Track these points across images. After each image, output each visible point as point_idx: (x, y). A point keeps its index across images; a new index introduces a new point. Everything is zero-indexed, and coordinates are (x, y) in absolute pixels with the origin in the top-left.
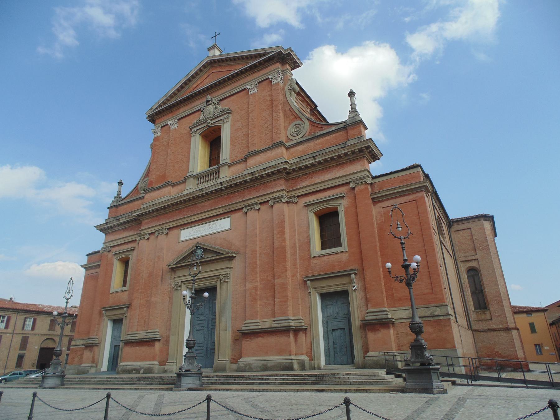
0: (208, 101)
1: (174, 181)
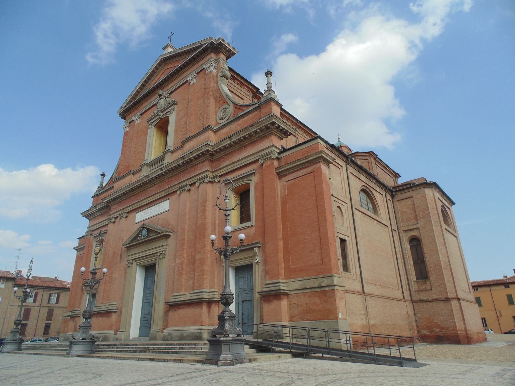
0: (160, 96)
1: (135, 169)
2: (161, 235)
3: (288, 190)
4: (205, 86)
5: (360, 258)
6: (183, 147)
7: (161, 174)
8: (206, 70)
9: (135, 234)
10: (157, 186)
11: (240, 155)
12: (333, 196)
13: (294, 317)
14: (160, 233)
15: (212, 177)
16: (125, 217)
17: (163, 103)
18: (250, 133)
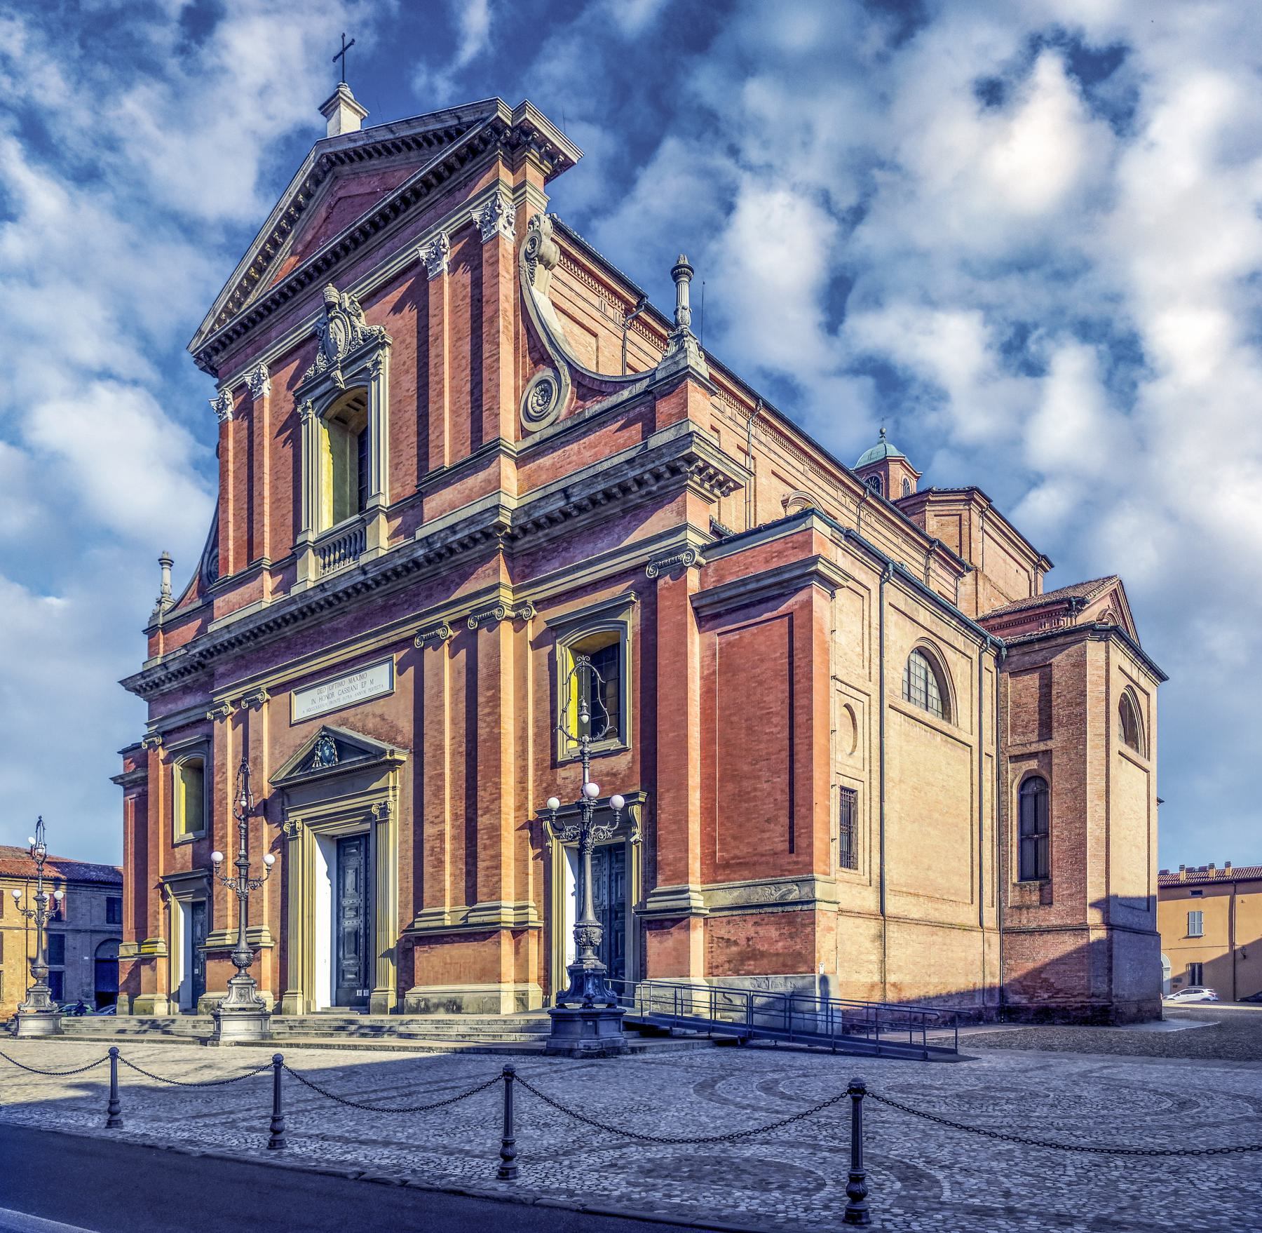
3: (720, 658)
5: (886, 834)
13: (717, 967)
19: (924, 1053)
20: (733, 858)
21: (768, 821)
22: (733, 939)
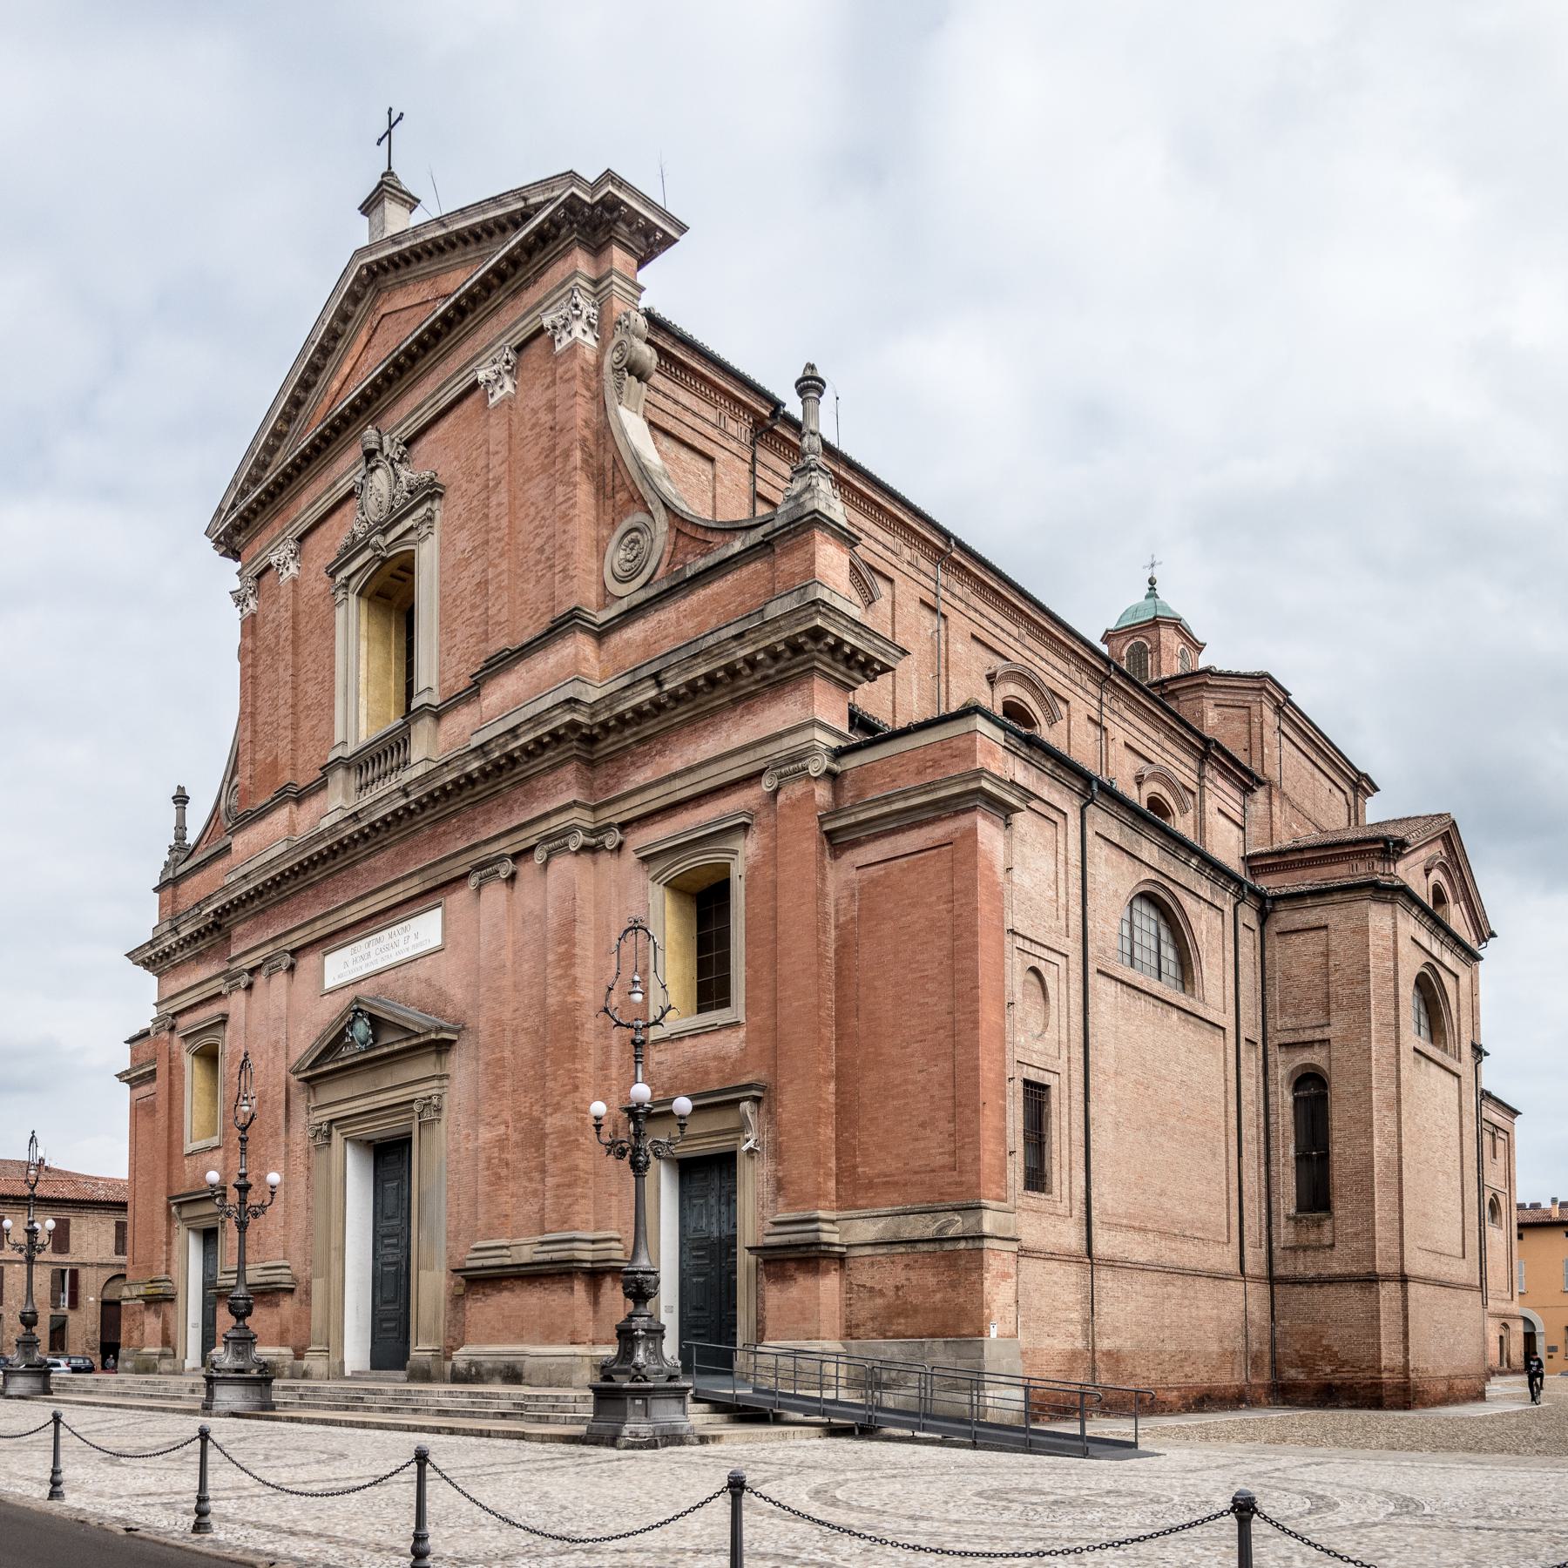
2: (422, 1040)
4: (550, 417)
6: (477, 693)
7: (406, 808)
8: (553, 337)
9: (330, 1034)
10: (390, 852)
11: (693, 746)
12: (1016, 933)
14: (418, 1035)
15: (591, 826)
16: (288, 970)
17: (385, 490)
18: (732, 664)
19: (1084, 1447)
20: (878, 1176)
21: (923, 1125)
22: (878, 1287)
